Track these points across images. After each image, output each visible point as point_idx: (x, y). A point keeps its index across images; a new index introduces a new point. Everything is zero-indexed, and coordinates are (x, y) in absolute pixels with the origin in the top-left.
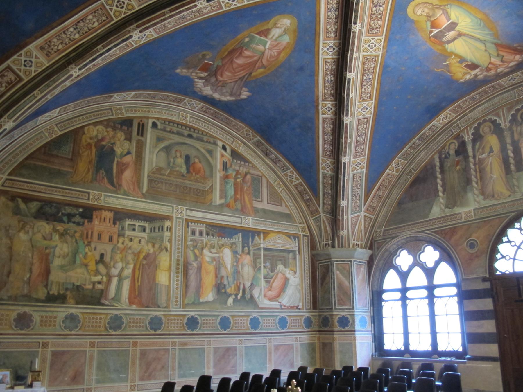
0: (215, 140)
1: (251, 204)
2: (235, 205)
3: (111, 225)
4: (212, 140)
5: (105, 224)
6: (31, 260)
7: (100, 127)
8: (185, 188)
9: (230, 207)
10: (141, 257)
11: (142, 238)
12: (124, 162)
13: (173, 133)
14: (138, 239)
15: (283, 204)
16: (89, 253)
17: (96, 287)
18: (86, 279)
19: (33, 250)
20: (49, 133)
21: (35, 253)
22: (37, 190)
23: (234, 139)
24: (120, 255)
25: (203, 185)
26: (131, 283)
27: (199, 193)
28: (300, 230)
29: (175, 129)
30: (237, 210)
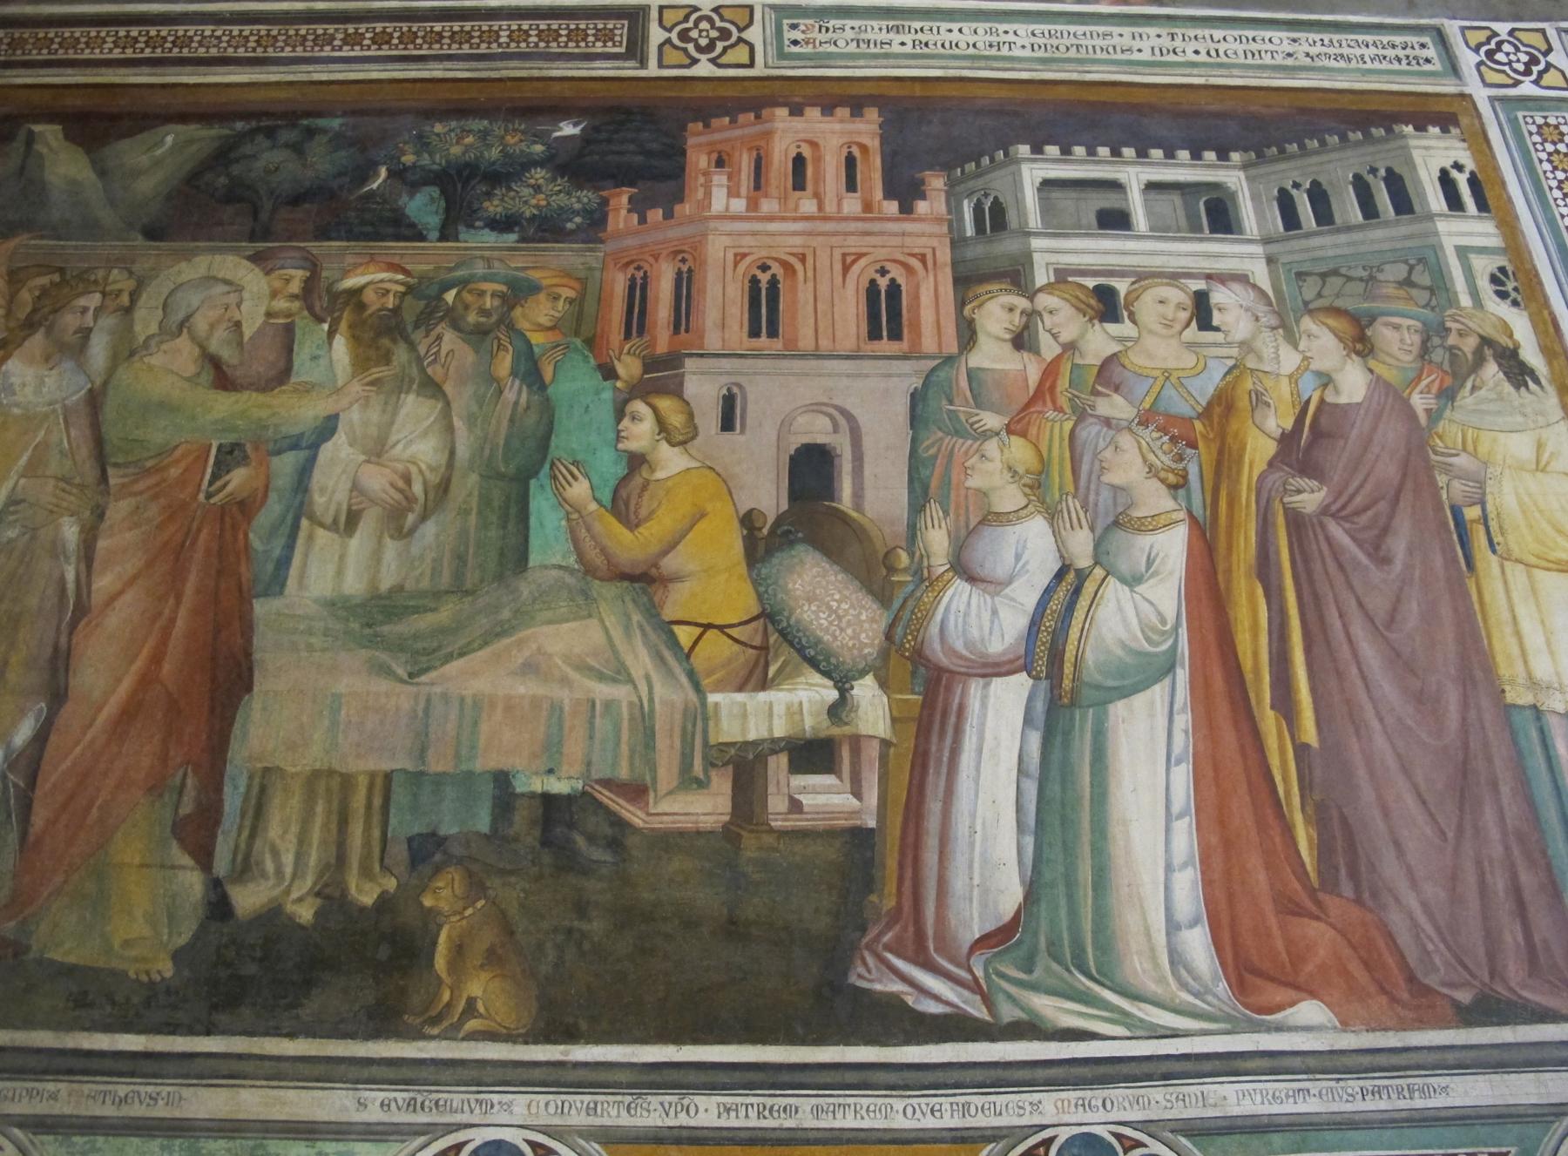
3: (867, 206)
5: (808, 206)
6: (70, 576)
10: (1259, 448)
11: (1223, 278)
14: (1177, 296)
16: (671, 462)
17: (777, 803)
18: (644, 723)
19: (104, 478)
21: (118, 510)
24: (1019, 451)
26: (1205, 724)
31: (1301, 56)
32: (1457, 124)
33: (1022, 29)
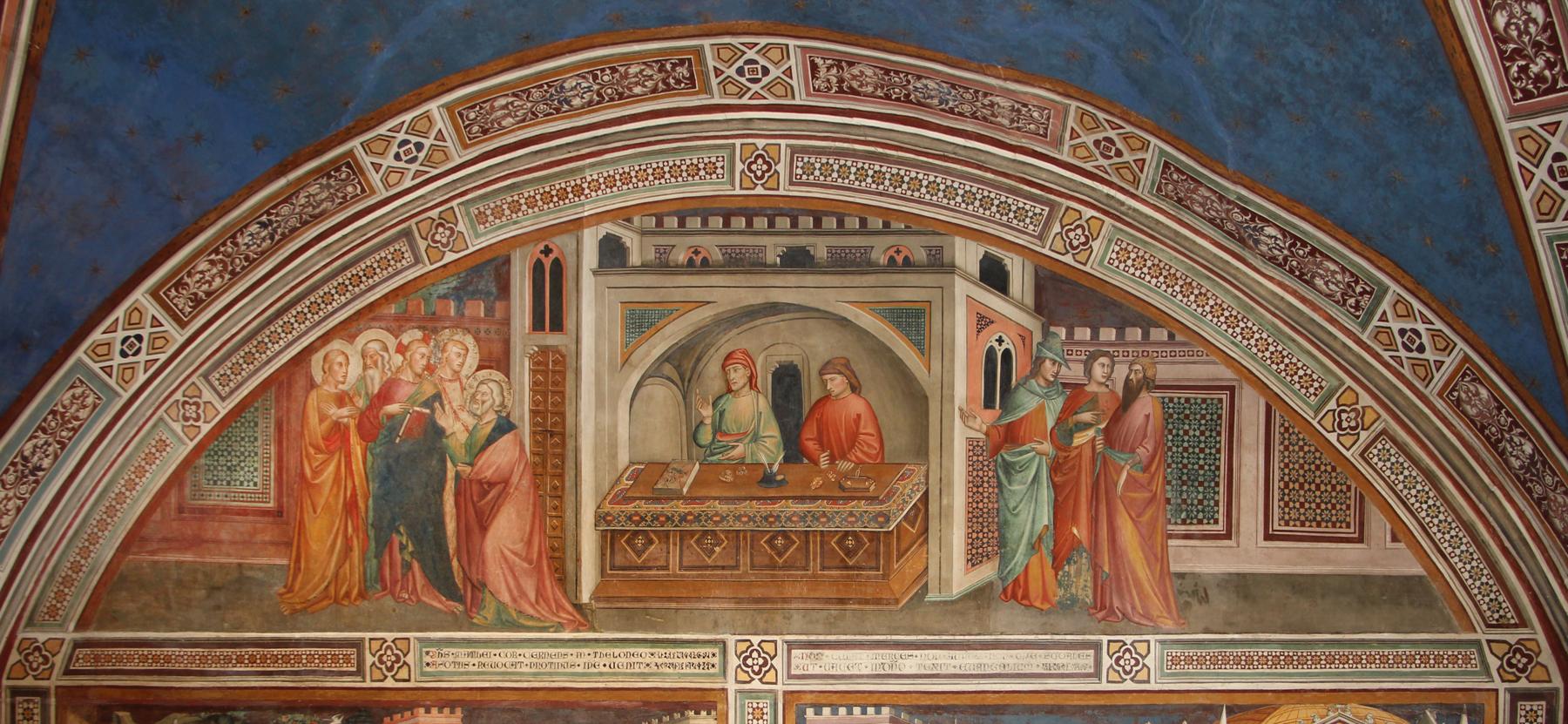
0: (935, 241)
1: (1159, 558)
2: (1060, 585)
4: (916, 248)
7: (372, 337)
8: (780, 542)
9: (1026, 596)
12: (488, 474)
13: (706, 267)
15: (1378, 525)
20: (186, 419)
22: (177, 667)
23: (1053, 206)
25: (878, 508)
27: (850, 553)
28: (1494, 663)
29: (712, 246)
30: (1068, 606)
31: (653, 665)
32: (716, 709)
33: (527, 652)
